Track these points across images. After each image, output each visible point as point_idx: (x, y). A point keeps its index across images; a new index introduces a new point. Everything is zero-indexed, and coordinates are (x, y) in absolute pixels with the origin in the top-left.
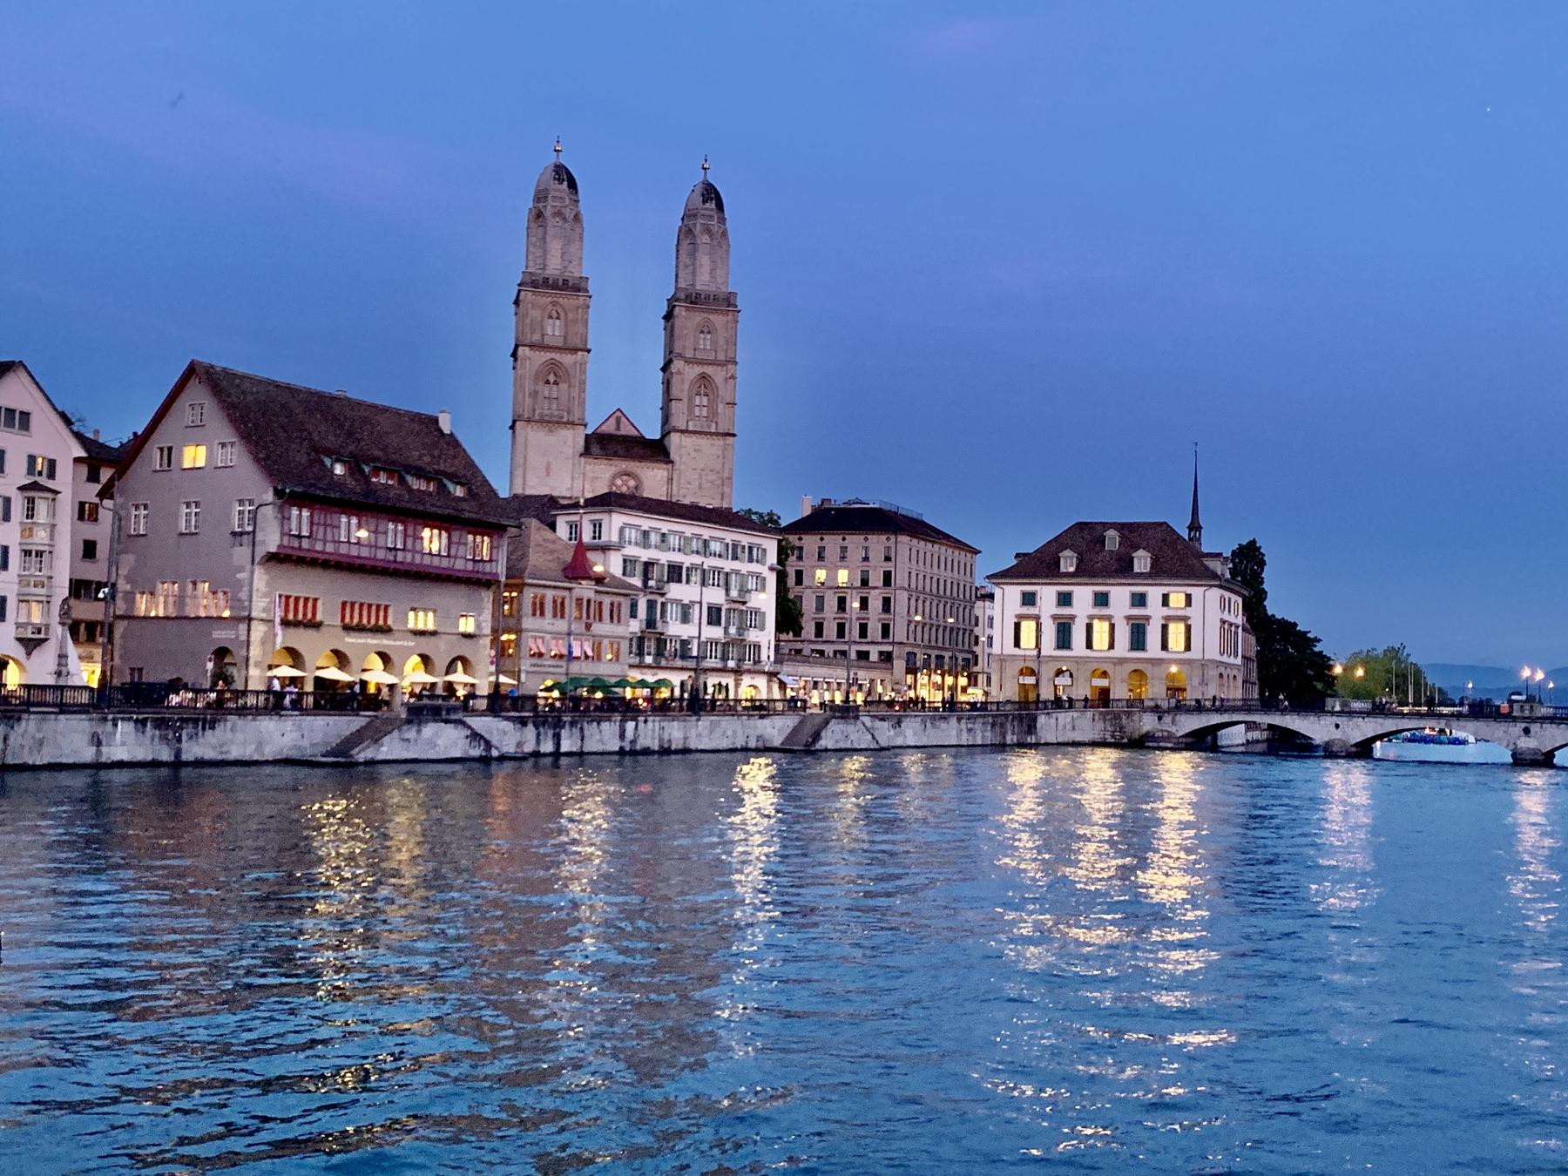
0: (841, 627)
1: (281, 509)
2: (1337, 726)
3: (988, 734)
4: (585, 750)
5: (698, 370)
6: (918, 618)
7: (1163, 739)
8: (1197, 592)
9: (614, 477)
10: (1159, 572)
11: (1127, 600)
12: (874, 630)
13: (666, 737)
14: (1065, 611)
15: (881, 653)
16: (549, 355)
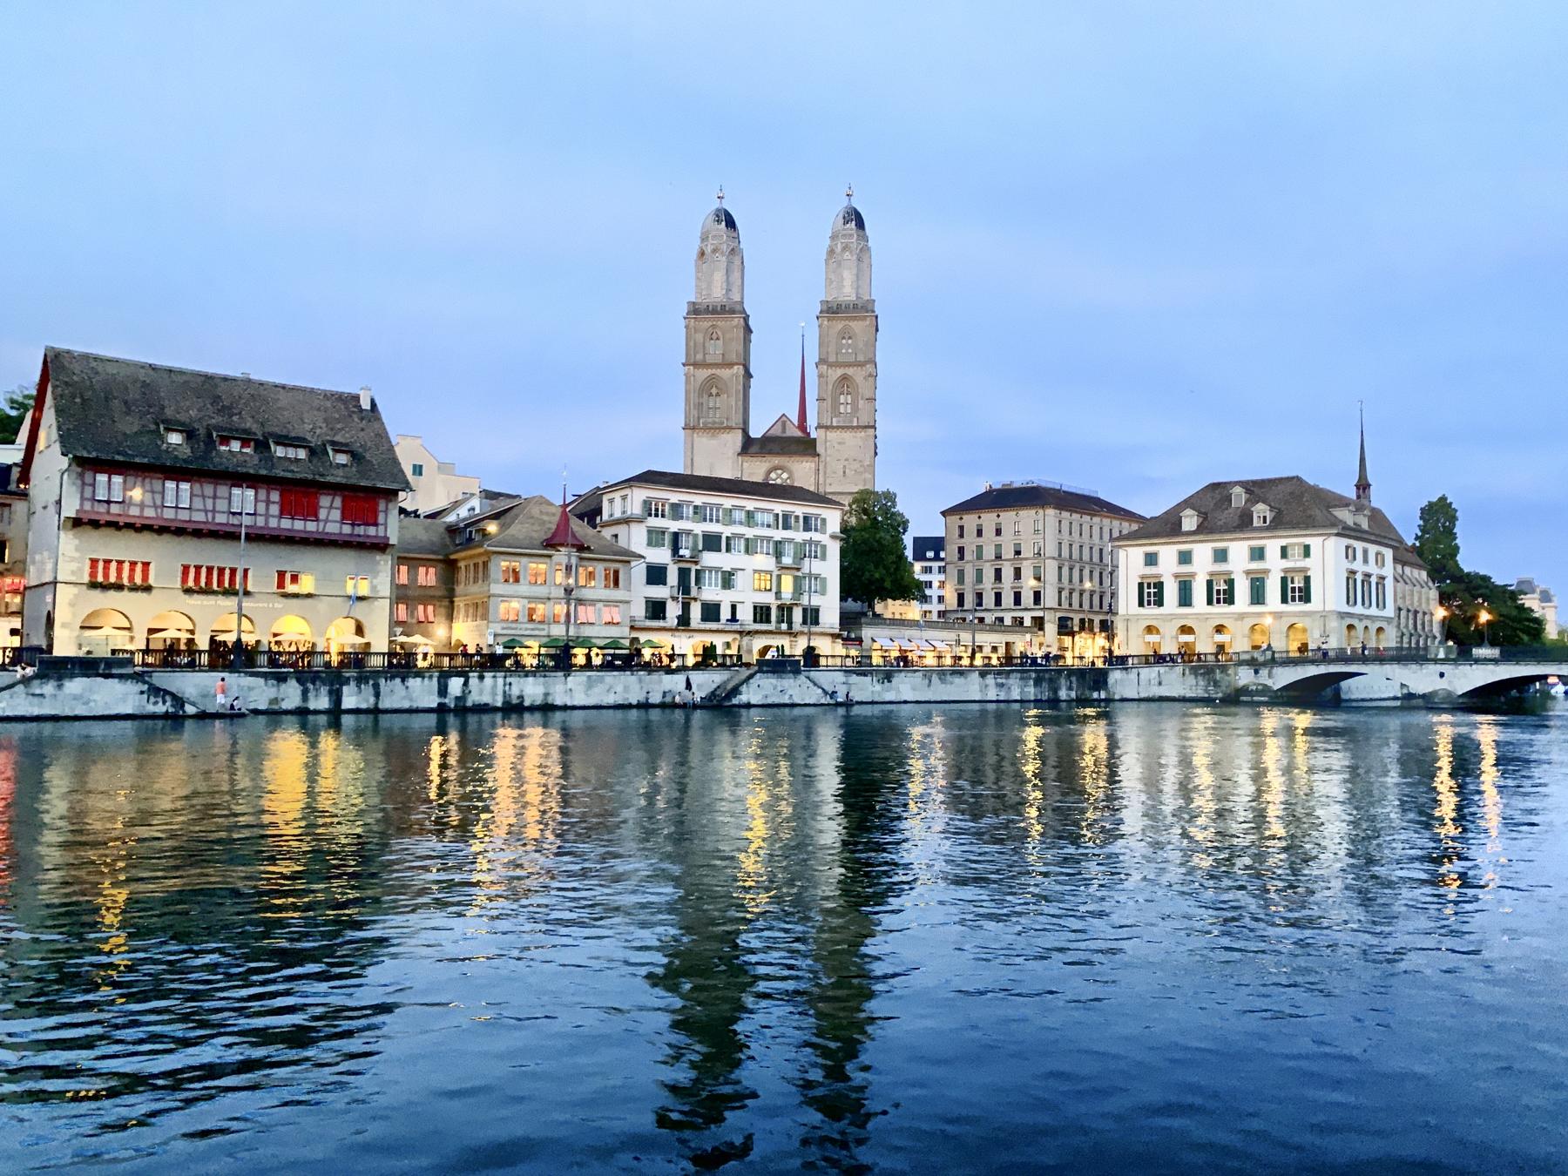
0: (998, 597)
1: (81, 476)
2: (1442, 675)
3: (1032, 690)
4: (381, 706)
5: (840, 372)
6: (1087, 585)
7: (1258, 693)
8: (1315, 543)
9: (769, 472)
10: (1279, 523)
11: (1246, 554)
12: (1027, 598)
13: (515, 691)
14: (1185, 569)
15: (1014, 618)
16: (710, 372)
